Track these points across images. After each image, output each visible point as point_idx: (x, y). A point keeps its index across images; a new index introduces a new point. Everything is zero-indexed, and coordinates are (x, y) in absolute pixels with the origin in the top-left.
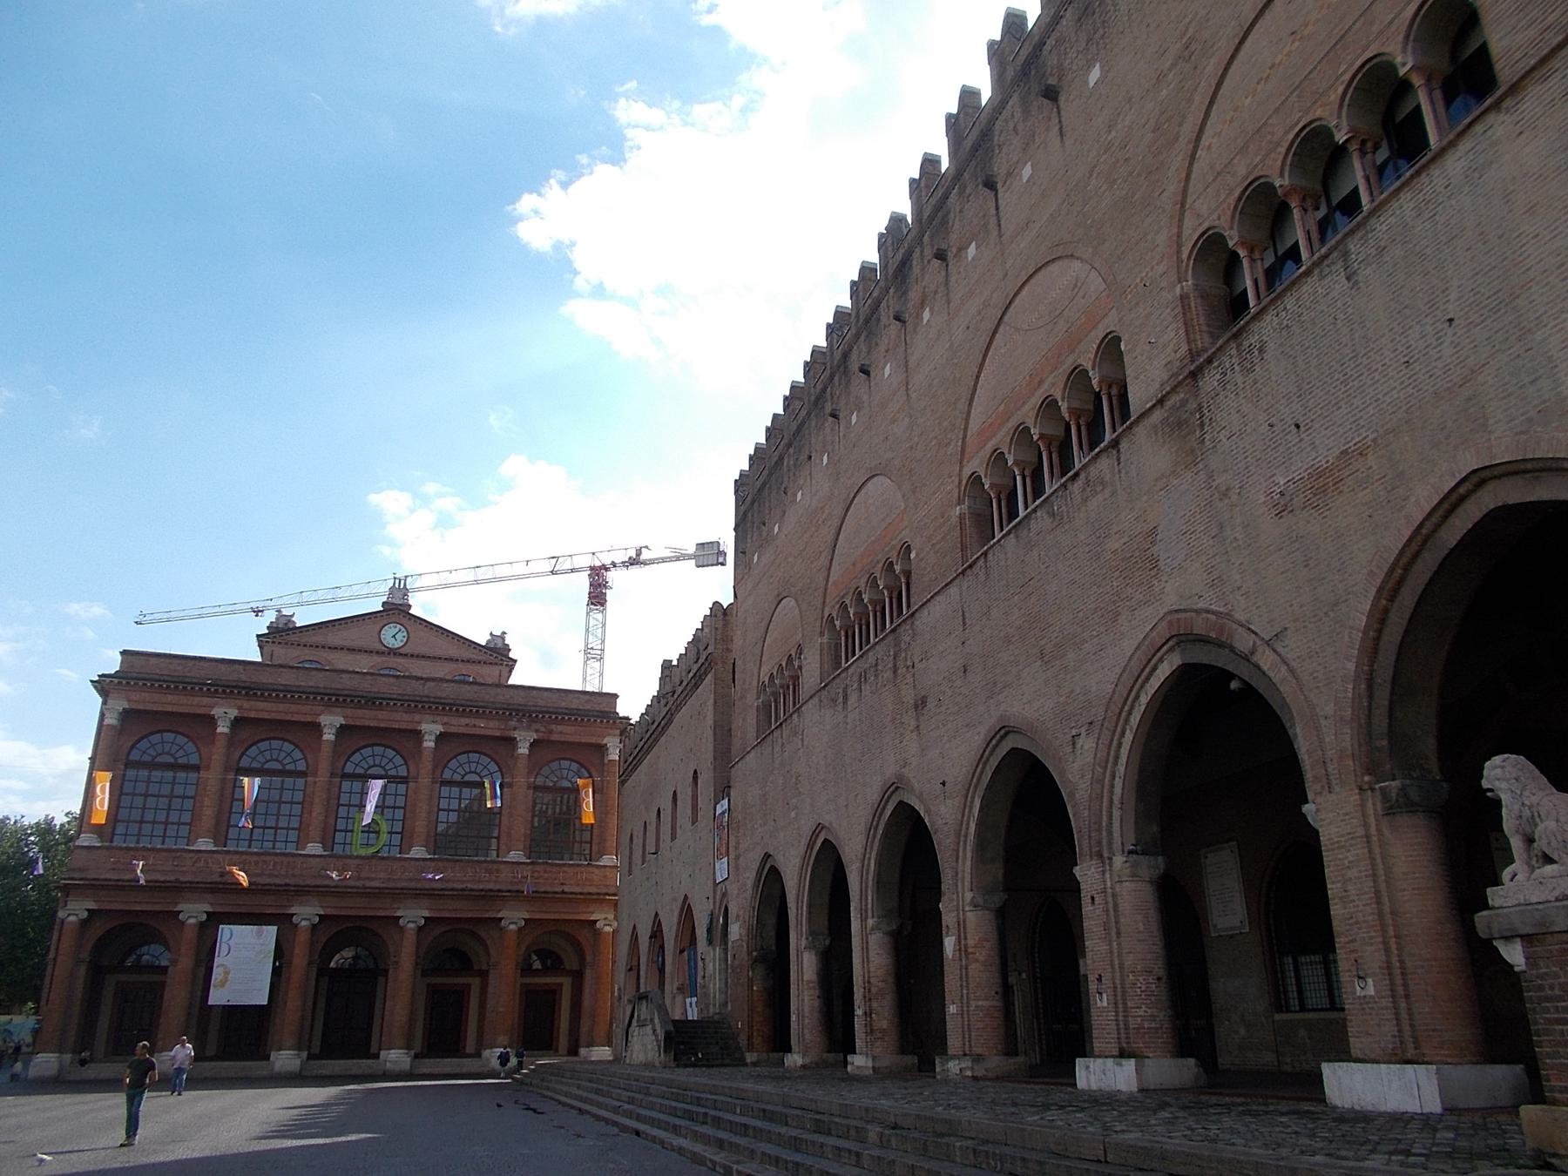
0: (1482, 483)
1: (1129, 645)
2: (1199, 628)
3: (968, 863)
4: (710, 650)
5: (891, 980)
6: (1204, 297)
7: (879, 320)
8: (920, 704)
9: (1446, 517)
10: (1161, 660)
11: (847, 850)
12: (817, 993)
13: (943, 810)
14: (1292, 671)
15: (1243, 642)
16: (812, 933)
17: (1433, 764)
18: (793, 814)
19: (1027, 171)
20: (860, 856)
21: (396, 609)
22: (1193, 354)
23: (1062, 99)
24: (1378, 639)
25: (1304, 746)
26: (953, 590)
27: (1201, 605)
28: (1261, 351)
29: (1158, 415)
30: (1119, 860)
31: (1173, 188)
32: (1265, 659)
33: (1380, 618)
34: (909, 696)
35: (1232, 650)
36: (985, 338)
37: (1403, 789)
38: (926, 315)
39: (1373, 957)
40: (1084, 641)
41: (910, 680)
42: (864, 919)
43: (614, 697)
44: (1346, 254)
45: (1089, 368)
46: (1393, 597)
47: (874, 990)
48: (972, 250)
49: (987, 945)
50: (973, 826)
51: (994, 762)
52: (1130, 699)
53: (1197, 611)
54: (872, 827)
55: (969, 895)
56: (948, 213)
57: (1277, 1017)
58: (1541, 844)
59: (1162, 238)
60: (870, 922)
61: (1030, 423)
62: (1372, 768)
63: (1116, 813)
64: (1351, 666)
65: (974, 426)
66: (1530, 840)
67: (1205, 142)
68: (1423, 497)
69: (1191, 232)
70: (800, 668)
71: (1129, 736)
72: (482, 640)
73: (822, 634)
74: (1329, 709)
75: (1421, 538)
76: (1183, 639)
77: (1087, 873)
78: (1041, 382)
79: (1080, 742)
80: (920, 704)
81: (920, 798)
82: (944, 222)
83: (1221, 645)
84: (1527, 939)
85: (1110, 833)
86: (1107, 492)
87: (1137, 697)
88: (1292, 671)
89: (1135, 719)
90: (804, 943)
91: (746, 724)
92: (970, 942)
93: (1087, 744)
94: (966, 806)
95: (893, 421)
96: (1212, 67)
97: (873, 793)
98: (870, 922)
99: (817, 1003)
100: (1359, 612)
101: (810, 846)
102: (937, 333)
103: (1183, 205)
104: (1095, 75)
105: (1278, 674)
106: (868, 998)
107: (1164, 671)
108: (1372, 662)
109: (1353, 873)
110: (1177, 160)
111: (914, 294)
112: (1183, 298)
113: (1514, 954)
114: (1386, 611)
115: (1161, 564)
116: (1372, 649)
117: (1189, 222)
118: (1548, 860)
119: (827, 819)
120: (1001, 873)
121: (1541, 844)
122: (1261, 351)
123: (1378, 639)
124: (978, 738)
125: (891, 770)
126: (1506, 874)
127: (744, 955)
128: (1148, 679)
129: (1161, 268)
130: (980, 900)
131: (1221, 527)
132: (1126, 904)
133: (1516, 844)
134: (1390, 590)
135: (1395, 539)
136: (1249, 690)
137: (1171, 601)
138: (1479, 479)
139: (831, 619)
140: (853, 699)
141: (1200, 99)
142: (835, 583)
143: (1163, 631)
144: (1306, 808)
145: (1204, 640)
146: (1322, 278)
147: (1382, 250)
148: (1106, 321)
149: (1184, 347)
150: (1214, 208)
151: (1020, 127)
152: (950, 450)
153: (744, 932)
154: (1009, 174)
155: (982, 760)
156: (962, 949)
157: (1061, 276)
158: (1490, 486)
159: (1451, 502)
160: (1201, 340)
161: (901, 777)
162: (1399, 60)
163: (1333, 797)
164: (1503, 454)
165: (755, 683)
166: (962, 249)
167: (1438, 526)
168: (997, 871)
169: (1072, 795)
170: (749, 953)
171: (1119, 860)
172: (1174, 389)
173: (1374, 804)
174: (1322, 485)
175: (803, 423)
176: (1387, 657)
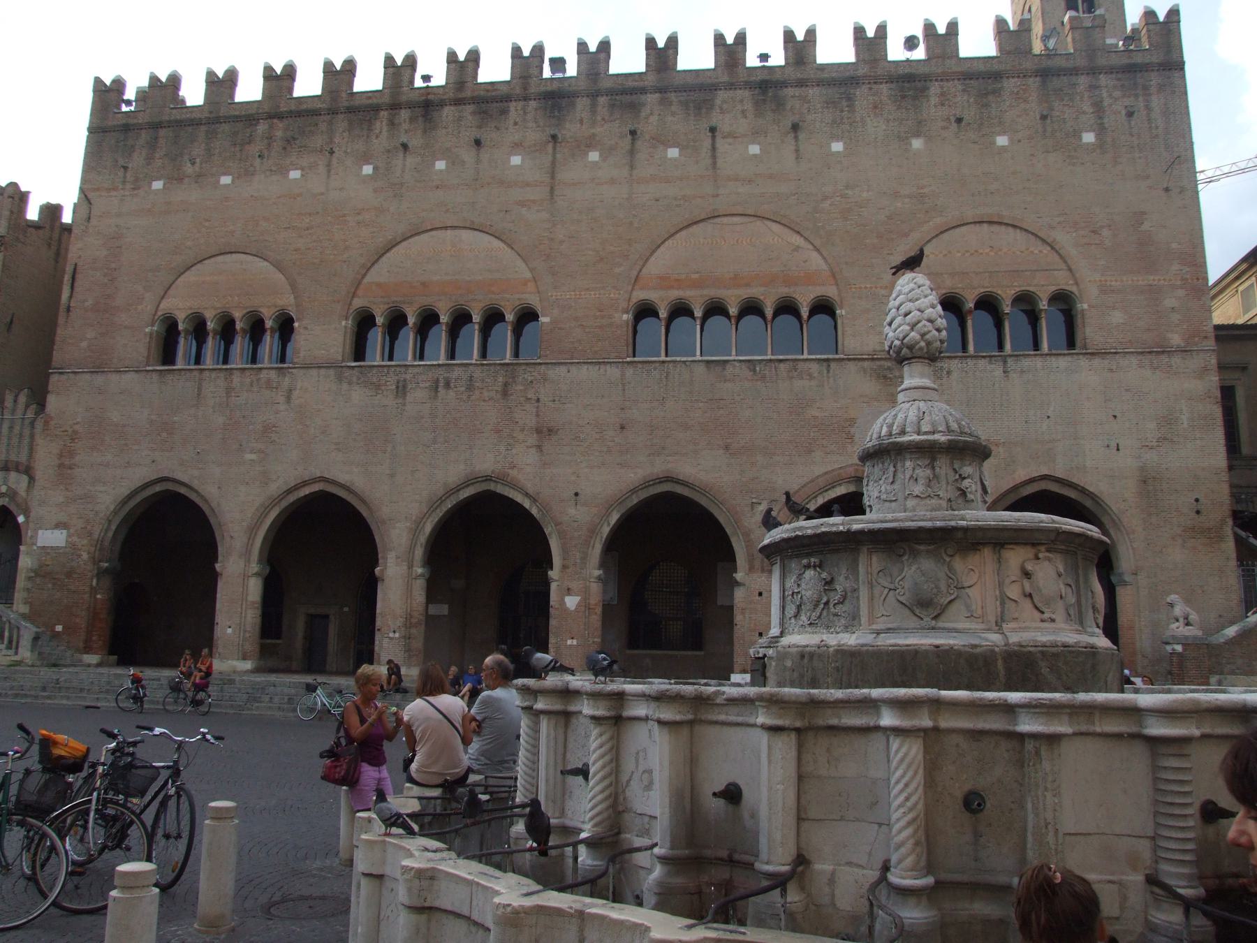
7: (504, 112)
23: (802, 136)
28: (949, 373)
44: (1005, 362)
50: (606, 530)
55: (598, 573)
66: (1186, 618)
75: (1015, 488)
86: (813, 383)
104: (837, 147)
146: (990, 363)
147: (1022, 372)
155: (634, 491)
157: (775, 235)
159: (1031, 481)
164: (1059, 474)
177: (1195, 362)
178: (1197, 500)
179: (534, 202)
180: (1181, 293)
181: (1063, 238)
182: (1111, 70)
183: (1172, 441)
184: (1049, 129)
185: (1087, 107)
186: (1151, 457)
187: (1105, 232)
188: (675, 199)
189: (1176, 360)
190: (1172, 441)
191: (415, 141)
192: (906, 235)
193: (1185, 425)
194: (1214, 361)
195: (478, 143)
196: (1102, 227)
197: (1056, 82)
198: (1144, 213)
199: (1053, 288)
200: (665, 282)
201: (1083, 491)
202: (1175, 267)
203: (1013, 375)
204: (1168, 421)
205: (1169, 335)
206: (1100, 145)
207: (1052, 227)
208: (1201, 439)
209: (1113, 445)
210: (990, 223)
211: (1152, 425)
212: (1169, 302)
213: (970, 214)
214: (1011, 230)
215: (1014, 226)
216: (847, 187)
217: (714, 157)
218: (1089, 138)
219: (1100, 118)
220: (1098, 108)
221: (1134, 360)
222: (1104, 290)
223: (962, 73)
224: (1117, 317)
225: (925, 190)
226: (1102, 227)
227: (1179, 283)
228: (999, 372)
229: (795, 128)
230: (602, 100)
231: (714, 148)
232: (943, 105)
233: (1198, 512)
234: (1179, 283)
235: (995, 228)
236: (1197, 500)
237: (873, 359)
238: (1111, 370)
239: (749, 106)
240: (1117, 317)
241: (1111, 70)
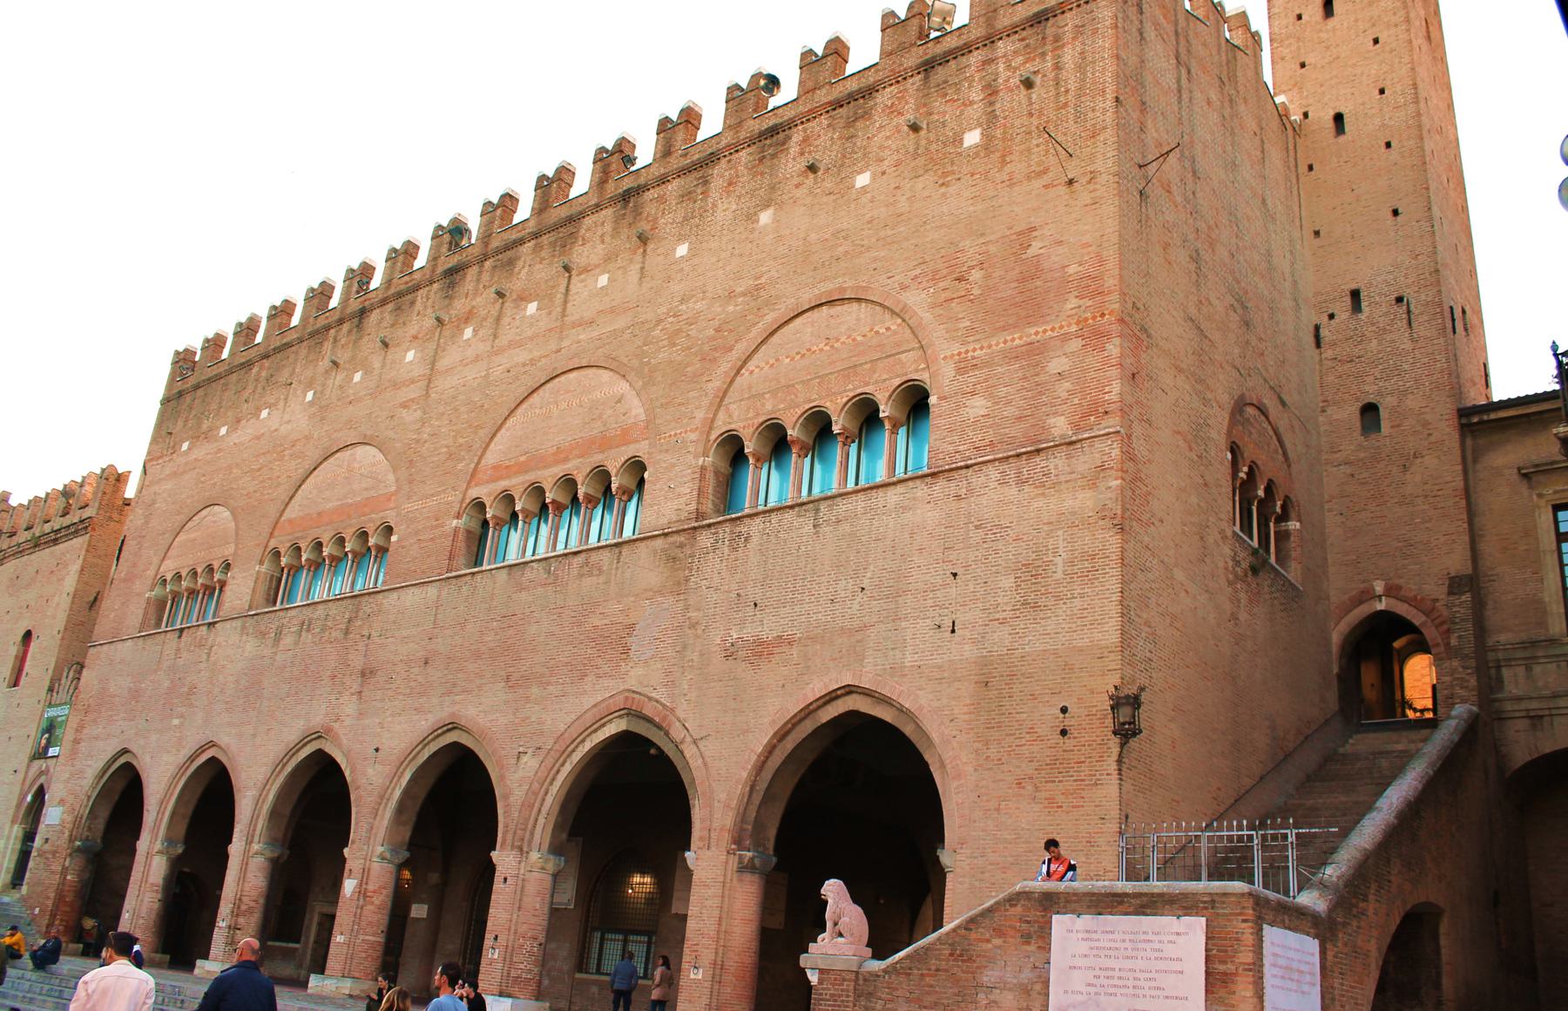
0: (850, 693)
1: (588, 702)
2: (647, 711)
3: (386, 822)
4: (88, 513)
5: (262, 901)
6: (716, 473)
7: (413, 303)
8: (366, 674)
9: (825, 704)
10: (610, 721)
11: (243, 776)
12: (160, 896)
13: (370, 771)
14: (705, 764)
15: (677, 732)
16: (169, 840)
17: (771, 845)
18: (176, 722)
19: (603, 280)
20: (260, 785)
22: (699, 515)
23: (651, 246)
24: (764, 762)
25: (697, 814)
26: (432, 591)
27: (653, 695)
28: (746, 539)
29: (659, 543)
30: (534, 855)
31: (717, 383)
32: (689, 751)
33: (770, 749)
34: (357, 661)
35: (667, 734)
36: (522, 391)
37: (752, 859)
38: (468, 333)
39: (707, 956)
40: (549, 683)
41: (361, 646)
42: (249, 842)
44: (817, 510)
45: (613, 473)
46: (780, 741)
47: (243, 907)
48: (532, 308)
49: (385, 892)
50: (398, 793)
51: (434, 747)
53: (650, 699)
54: (282, 763)
55: (380, 849)
56: (518, 258)
57: (578, 975)
58: (840, 927)
59: (700, 414)
60: (256, 847)
61: (547, 486)
62: (738, 841)
63: (541, 821)
64: (745, 774)
65: (491, 458)
67: (751, 365)
68: (817, 687)
69: (721, 427)
70: (223, 584)
71: (568, 767)
73: (261, 563)
74: (723, 796)
75: (808, 712)
77: (503, 858)
78: (566, 460)
79: (525, 759)
80: (366, 674)
81: (347, 756)
82: (511, 263)
83: (659, 727)
84: (822, 971)
85: (532, 834)
86: (602, 579)
87: (583, 741)
88: (705, 764)
89: (577, 757)
90: (158, 846)
91: (126, 606)
92: (371, 887)
93: (530, 763)
94: (396, 774)
95: (404, 406)
96: (770, 318)
97: (292, 735)
98: (256, 847)
99: (157, 905)
100: (760, 741)
101: (192, 758)
102: (472, 355)
103: (722, 400)
104: (682, 250)
105: (695, 763)
106: (236, 913)
108: (758, 774)
109: (709, 903)
110: (725, 366)
111: (460, 305)
112: (703, 468)
113: (813, 978)
114: (774, 747)
115: (631, 653)
116: (760, 767)
117: (721, 415)
118: (841, 935)
119: (224, 739)
120: (408, 835)
121: (840, 927)
122: (746, 539)
123: (764, 762)
124: (425, 724)
125: (317, 720)
126: (820, 937)
127: (63, 842)
128: (595, 731)
129: (693, 436)
130: (388, 855)
131: (685, 647)
132: (531, 888)
133: (829, 925)
134: (781, 735)
135: (794, 708)
136: (663, 758)
137: (632, 683)
138: (849, 690)
139: (277, 554)
140: (288, 640)
141: (756, 333)
142: (290, 521)
143: (619, 702)
144: (687, 854)
145: (649, 720)
148: (637, 446)
149: (693, 506)
150: (745, 422)
151: (607, 239)
152: (460, 467)
153: (69, 818)
154: (586, 270)
155: (424, 742)
156: (361, 892)
157: (607, 385)
158: (854, 696)
159: (831, 697)
160: (708, 506)
161: (329, 730)
162: (882, 408)
163: (708, 853)
165: (151, 573)
166: (523, 299)
167: (819, 708)
168: (406, 833)
169: (506, 797)
170: (71, 840)
171: (534, 855)
172: (677, 532)
173: (733, 863)
174: (761, 650)
175: (289, 345)
176: (768, 774)
177: (1085, 460)
178: (1064, 710)
179: (412, 400)
180: (1075, 345)
181: (917, 300)
182: (1013, 30)
183: (1036, 607)
184: (923, 142)
185: (976, 94)
186: (1000, 637)
187: (976, 275)
188: (524, 365)
189: (1056, 463)
190: (1036, 607)
191: (343, 356)
192: (731, 349)
193: (1059, 575)
194: (1116, 452)
195: (385, 345)
196: (973, 267)
197: (940, 73)
198: (1033, 229)
199: (897, 382)
200: (500, 471)
201: (901, 710)
202: (1073, 303)
203: (826, 529)
204: (1032, 571)
205: (1052, 421)
206: (987, 146)
207: (904, 288)
208: (1082, 596)
209: (948, 624)
210: (829, 303)
211: (1008, 582)
212: (1057, 364)
213: (807, 297)
214: (855, 305)
215: (859, 300)
216: (682, 301)
217: (566, 302)
218: (972, 138)
219: (991, 104)
220: (991, 91)
221: (993, 472)
222: (964, 366)
223: (830, 103)
224: (978, 406)
225: (763, 280)
226: (973, 267)
227: (1074, 328)
228: (809, 528)
229: (643, 239)
230: (488, 264)
231: (567, 289)
232: (802, 154)
233: (1064, 733)
234: (1074, 328)
235: (837, 309)
236: (1064, 710)
237: (666, 535)
238: (958, 497)
239: (608, 227)
240: (978, 406)
241: (1013, 30)
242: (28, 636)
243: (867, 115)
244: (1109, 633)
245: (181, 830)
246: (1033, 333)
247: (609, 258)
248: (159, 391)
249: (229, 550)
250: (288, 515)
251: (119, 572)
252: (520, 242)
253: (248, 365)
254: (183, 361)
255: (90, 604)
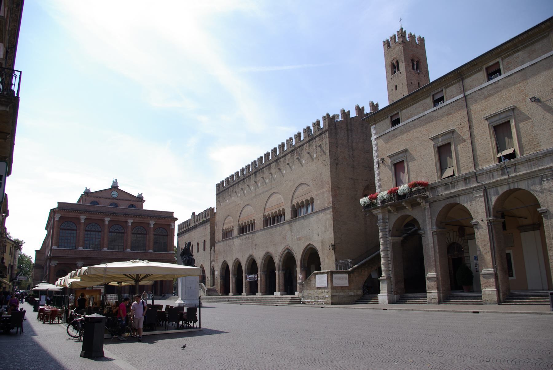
4: (209, 217)
8: (256, 245)
21: (115, 187)
43: (173, 213)
52: (283, 254)
59: (290, 202)
68: (307, 244)
72: (136, 195)
76: (288, 249)
80: (256, 245)
91: (219, 235)
107: (286, 252)
125: (251, 253)
138: (310, 244)
156: (261, 280)
174: (299, 239)
212: (326, 195)
222: (317, 195)
242: (205, 241)
243: (302, 149)
244: (332, 235)
245: (236, 273)
246: (323, 190)
247: (276, 172)
248: (215, 193)
249: (233, 224)
250: (241, 217)
251: (217, 229)
252: (264, 168)
253: (229, 188)
254: (218, 186)
255: (213, 234)
